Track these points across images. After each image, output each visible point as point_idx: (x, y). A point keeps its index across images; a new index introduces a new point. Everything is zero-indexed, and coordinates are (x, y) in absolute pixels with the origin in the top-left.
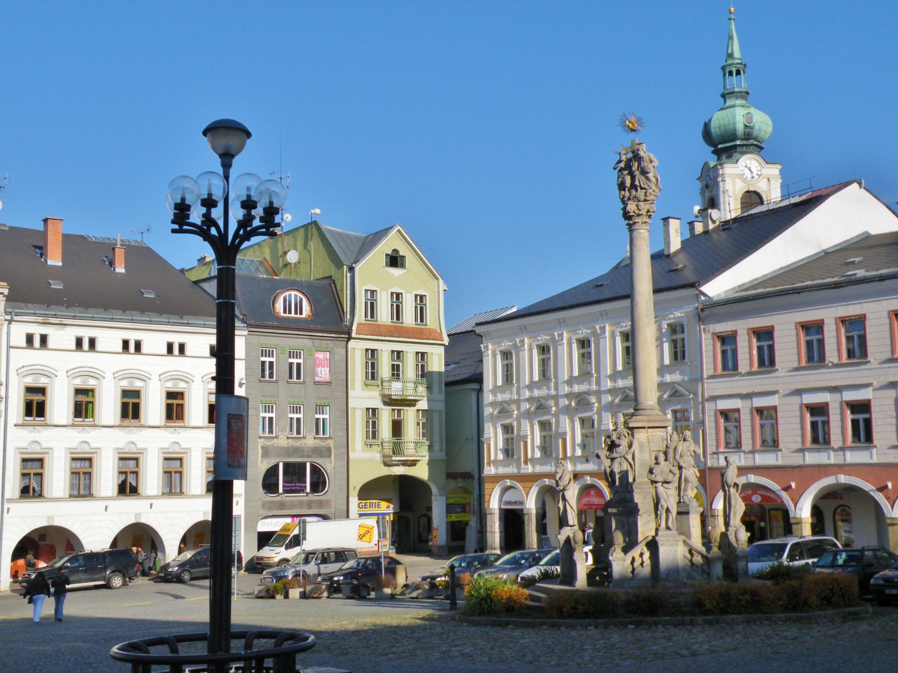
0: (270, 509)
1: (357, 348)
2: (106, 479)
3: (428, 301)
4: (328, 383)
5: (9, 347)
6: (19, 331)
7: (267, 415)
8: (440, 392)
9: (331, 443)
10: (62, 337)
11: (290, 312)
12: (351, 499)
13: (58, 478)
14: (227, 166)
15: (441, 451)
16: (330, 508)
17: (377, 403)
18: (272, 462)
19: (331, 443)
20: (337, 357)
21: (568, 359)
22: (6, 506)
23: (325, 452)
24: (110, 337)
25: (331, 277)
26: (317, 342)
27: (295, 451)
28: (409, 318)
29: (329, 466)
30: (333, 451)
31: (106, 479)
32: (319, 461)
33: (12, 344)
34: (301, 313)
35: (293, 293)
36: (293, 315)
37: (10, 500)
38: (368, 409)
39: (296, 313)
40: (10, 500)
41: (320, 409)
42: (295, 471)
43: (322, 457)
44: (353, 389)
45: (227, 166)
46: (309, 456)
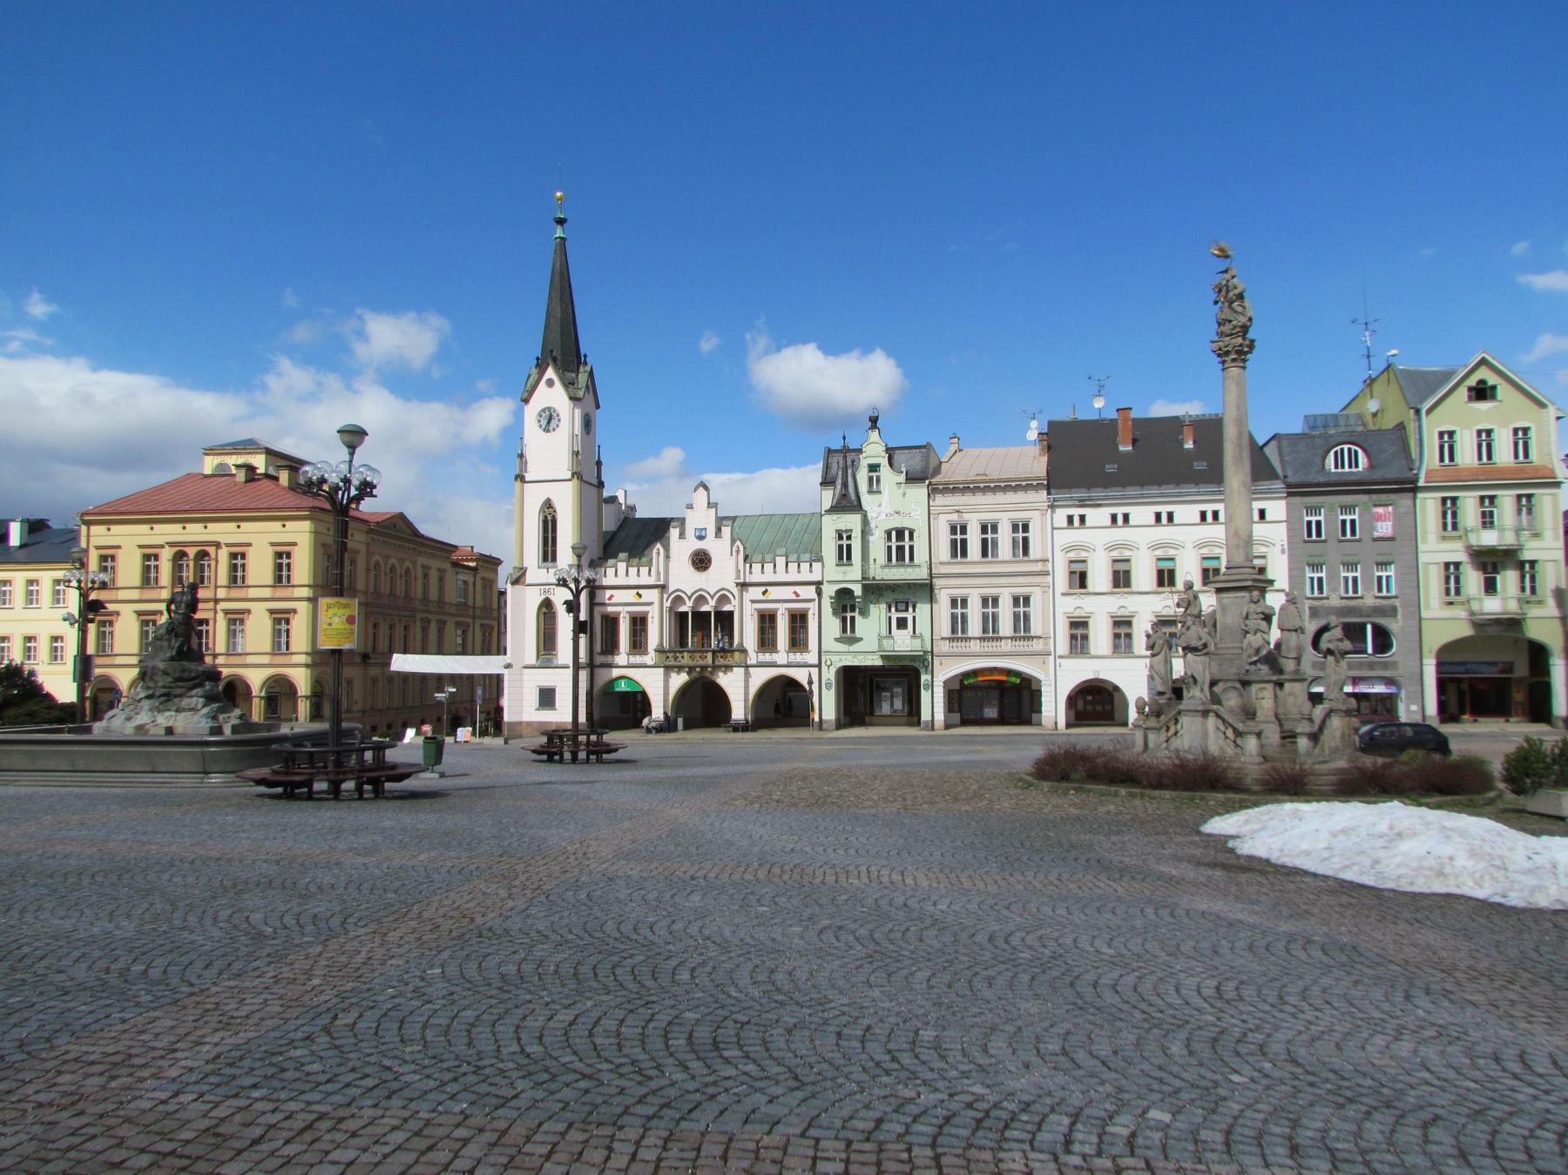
3: (1532, 434)
4: (1392, 539)
6: (1061, 515)
7: (1316, 575)
8: (1556, 538)
10: (1098, 516)
12: (1425, 661)
13: (1100, 635)
14: (352, 454)
17: (1461, 557)
19: (1396, 602)
23: (1392, 612)
24: (1142, 514)
26: (1375, 497)
28: (1503, 454)
29: (1394, 626)
35: (1346, 447)
36: (1347, 469)
38: (1447, 565)
41: (1383, 565)
44: (1425, 541)
45: (352, 454)
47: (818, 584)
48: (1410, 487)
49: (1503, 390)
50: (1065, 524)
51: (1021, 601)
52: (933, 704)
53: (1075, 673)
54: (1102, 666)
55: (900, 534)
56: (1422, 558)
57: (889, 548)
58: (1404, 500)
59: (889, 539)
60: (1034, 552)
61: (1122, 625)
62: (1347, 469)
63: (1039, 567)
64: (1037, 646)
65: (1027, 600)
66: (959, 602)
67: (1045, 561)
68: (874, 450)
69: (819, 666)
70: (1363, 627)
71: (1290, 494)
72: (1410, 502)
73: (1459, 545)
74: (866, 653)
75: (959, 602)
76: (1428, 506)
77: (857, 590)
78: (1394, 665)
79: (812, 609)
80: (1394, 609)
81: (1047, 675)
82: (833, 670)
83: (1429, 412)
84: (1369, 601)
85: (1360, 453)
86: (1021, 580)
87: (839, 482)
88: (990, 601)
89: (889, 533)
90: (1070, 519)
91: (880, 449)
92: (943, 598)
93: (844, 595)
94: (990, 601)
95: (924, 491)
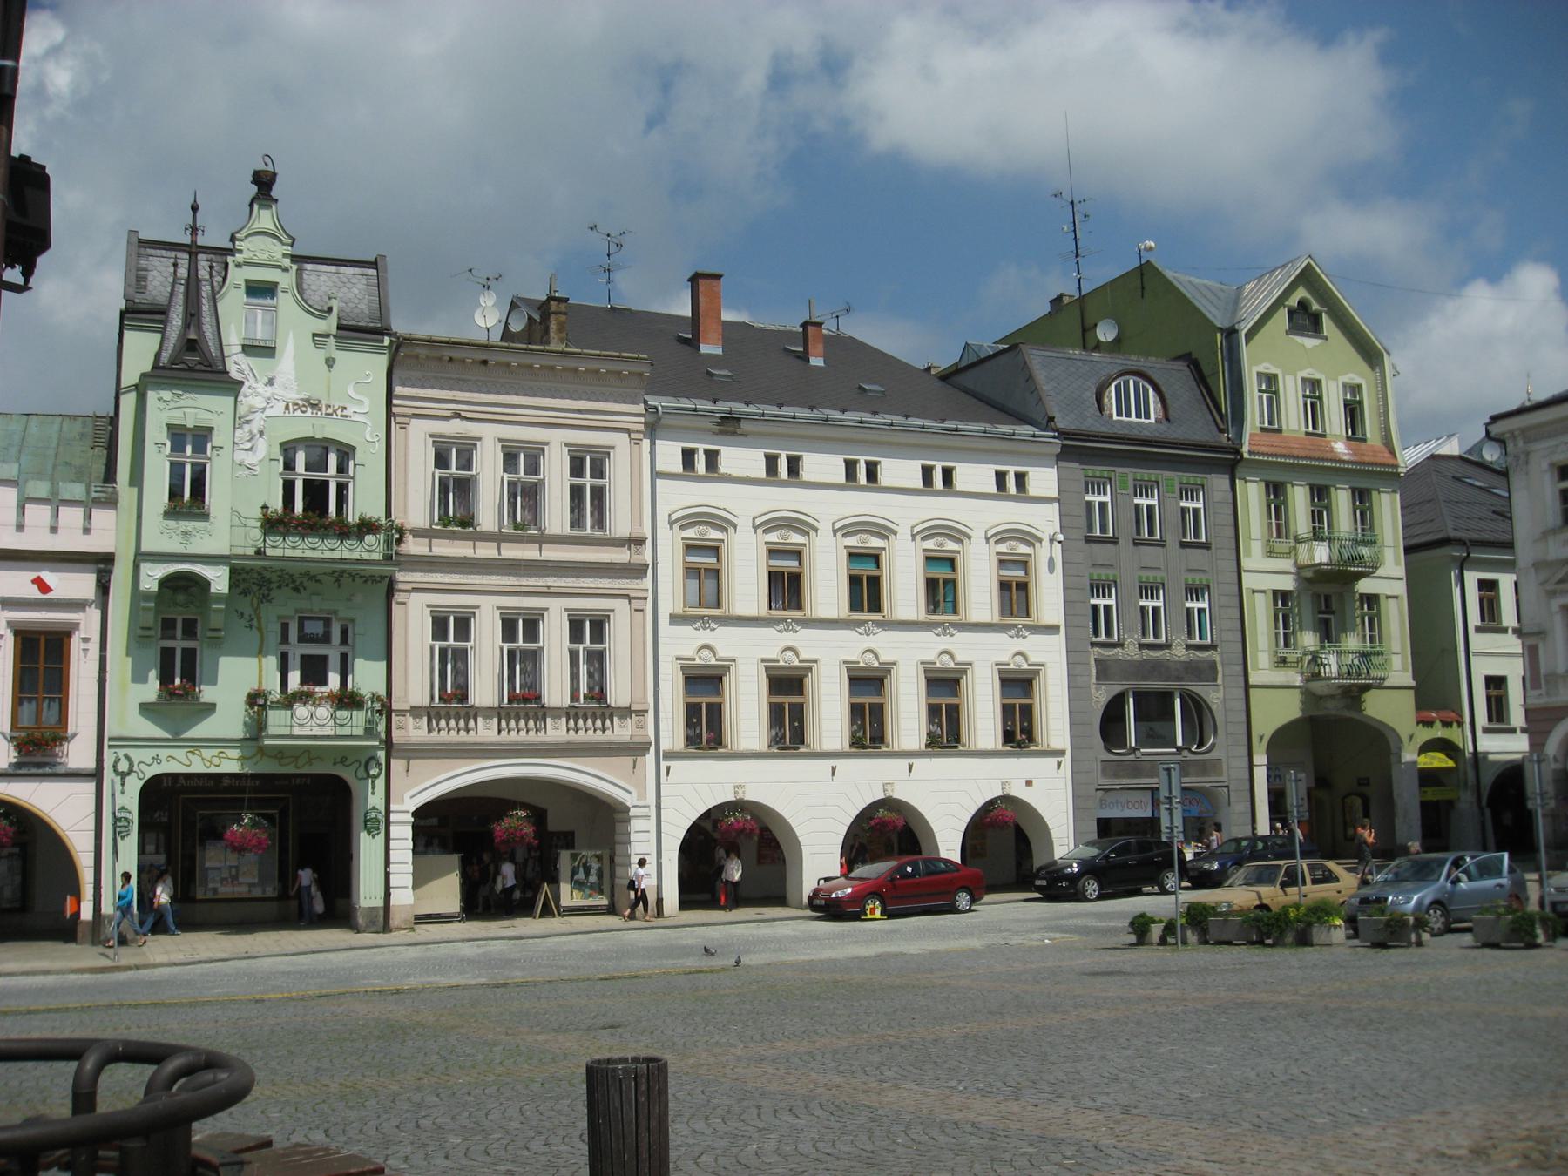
0: (1116, 776)
2: (829, 713)
5: (656, 475)
8: (1397, 563)
9: (1215, 656)
11: (1128, 415)
13: (747, 712)
15: (1405, 670)
16: (1221, 774)
18: (1117, 689)
19: (1215, 656)
20: (1218, 496)
22: (664, 765)
23: (1207, 672)
25: (1190, 354)
27: (1155, 669)
29: (1214, 695)
30: (1220, 669)
31: (829, 713)
32: (1198, 688)
33: (659, 467)
34: (1147, 416)
37: (671, 755)
38: (1275, 592)
39: (1138, 416)
40: (671, 755)
41: (1194, 591)
42: (1155, 708)
43: (1200, 680)
44: (1249, 555)
46: (1179, 679)
47: (102, 563)
48: (1231, 463)
49: (1326, 321)
50: (678, 467)
51: (588, 629)
52: (386, 865)
53: (696, 788)
54: (749, 776)
55: (319, 449)
56: (1248, 581)
57: (289, 487)
58: (1219, 482)
59: (289, 466)
60: (620, 522)
61: (787, 685)
62: (1133, 418)
63: (621, 556)
64: (622, 731)
65: (599, 627)
66: (451, 627)
67: (640, 542)
68: (261, 251)
69: (96, 775)
70: (1167, 697)
71: (1066, 454)
73: (1287, 565)
74: (214, 747)
75: (451, 627)
76: (1252, 493)
77: (219, 580)
78: (1206, 767)
79: (89, 622)
80: (1213, 665)
81: (642, 796)
82: (134, 786)
83: (1250, 335)
84: (1179, 653)
85: (1151, 391)
86: (587, 583)
87: (176, 319)
88: (521, 628)
89: (288, 449)
90: (688, 456)
91: (277, 251)
92: (413, 620)
93: (184, 587)
94: (521, 628)
95: (382, 361)
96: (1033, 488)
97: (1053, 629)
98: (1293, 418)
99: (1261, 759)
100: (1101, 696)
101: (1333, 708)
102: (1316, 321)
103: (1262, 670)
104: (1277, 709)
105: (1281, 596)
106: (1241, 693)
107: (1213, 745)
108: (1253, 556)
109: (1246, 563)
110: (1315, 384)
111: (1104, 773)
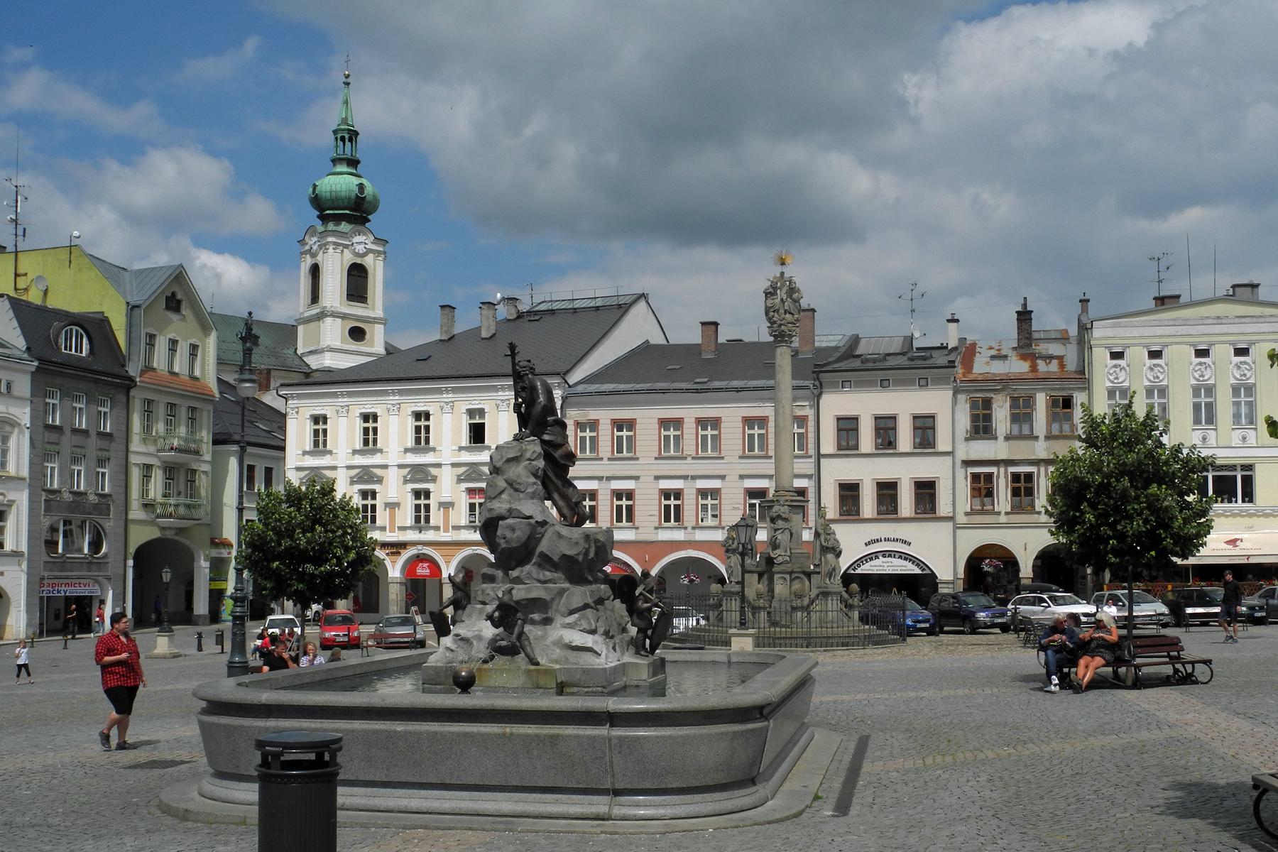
1: (137, 396)
21: (396, 430)
29: (110, 524)
56: (134, 459)
72: (124, 399)
96: (16, 390)
97: (24, 479)
98: (159, 360)
99: (131, 563)
100: (46, 522)
101: (169, 534)
102: (179, 302)
103: (136, 513)
104: (140, 536)
105: (148, 468)
106: (122, 524)
107: (105, 556)
108: (136, 445)
109: (133, 448)
110: (173, 343)
111: (45, 568)
